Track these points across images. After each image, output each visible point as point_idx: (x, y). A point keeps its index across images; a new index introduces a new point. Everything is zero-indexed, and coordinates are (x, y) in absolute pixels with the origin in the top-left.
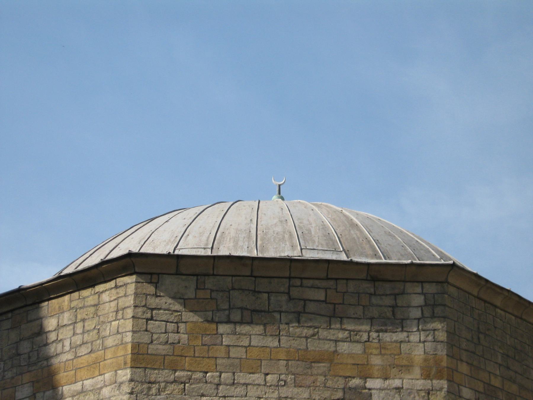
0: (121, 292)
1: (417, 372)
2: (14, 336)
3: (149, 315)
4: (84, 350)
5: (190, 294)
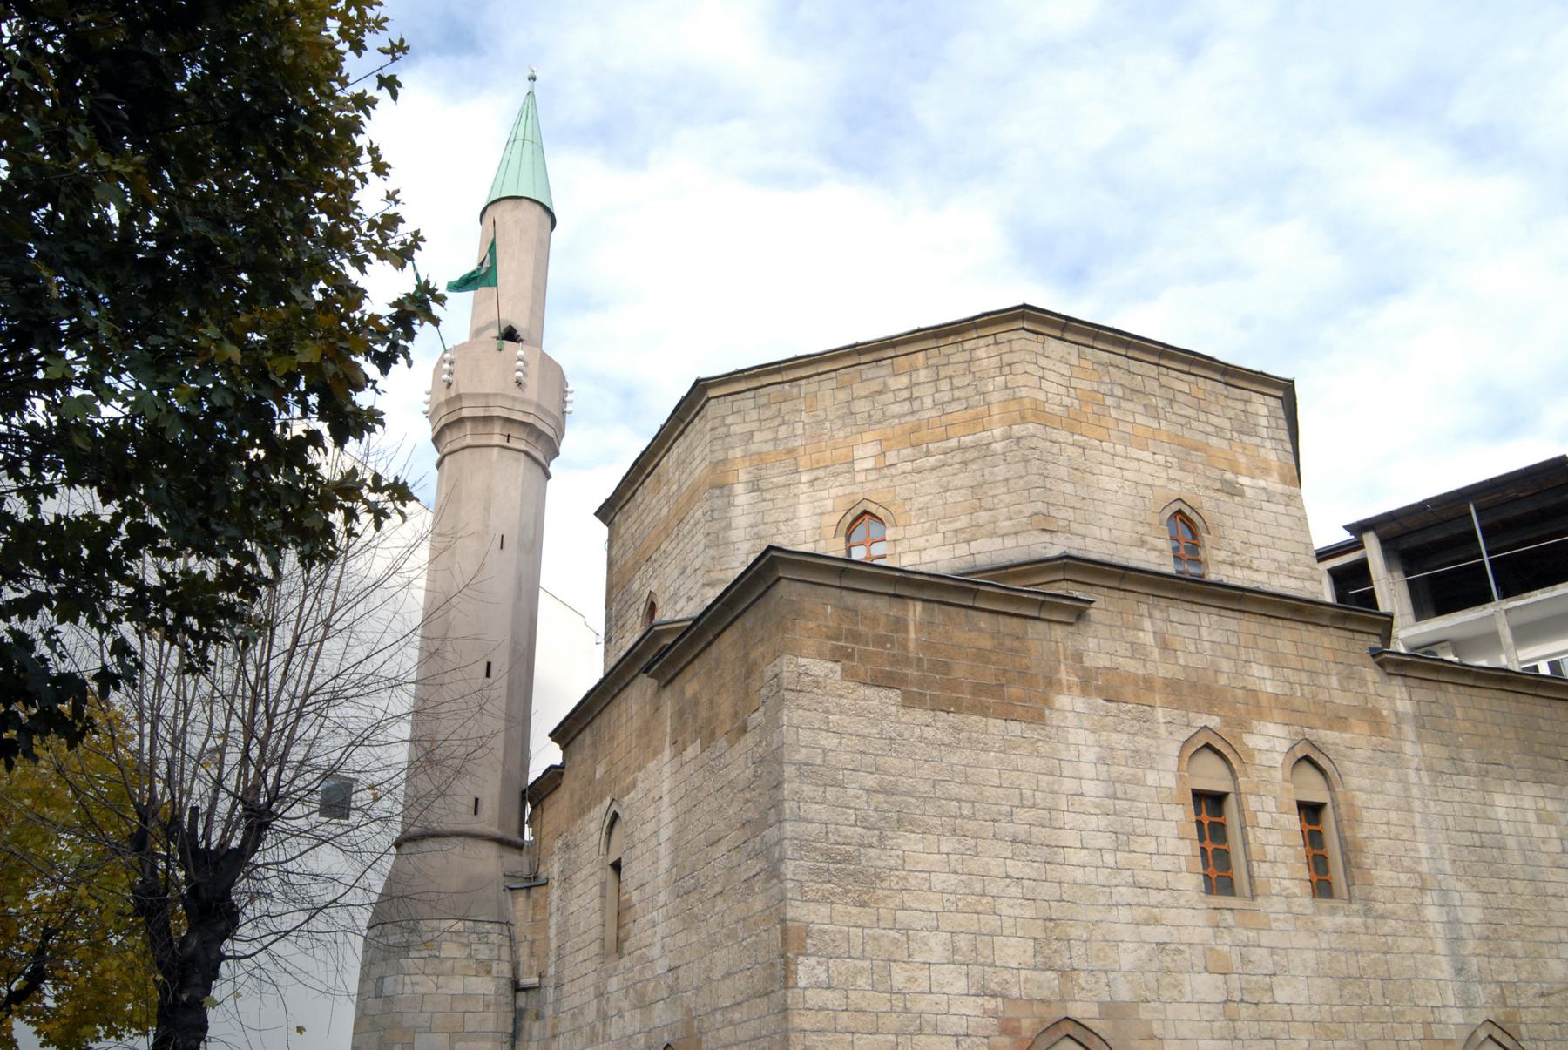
0: (1005, 348)
1: (1275, 475)
2: (842, 395)
3: (1041, 374)
4: (955, 407)
5: (1074, 360)
